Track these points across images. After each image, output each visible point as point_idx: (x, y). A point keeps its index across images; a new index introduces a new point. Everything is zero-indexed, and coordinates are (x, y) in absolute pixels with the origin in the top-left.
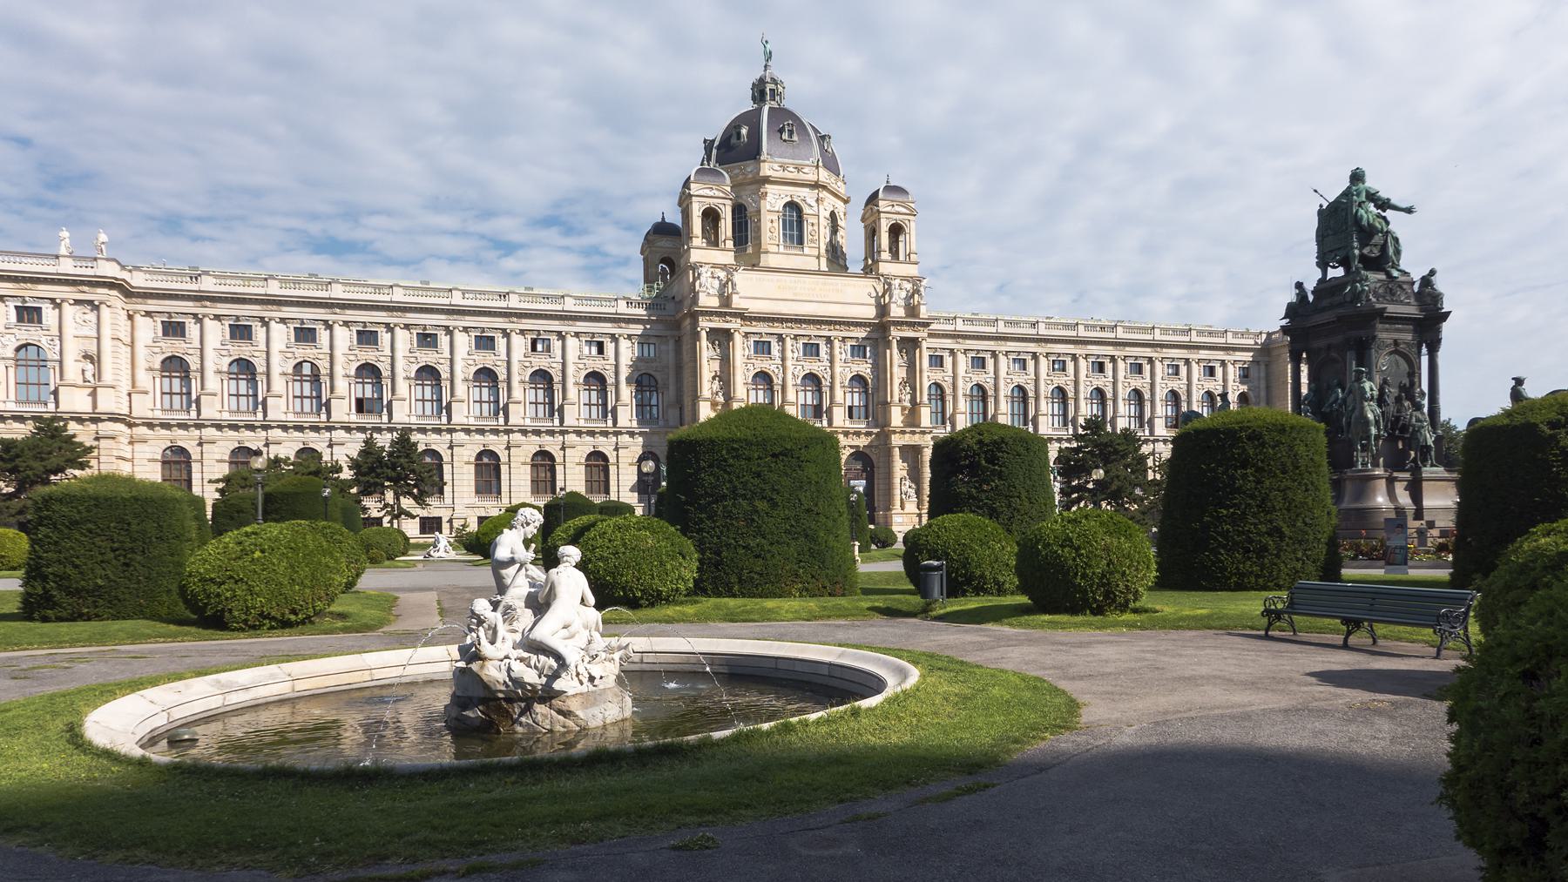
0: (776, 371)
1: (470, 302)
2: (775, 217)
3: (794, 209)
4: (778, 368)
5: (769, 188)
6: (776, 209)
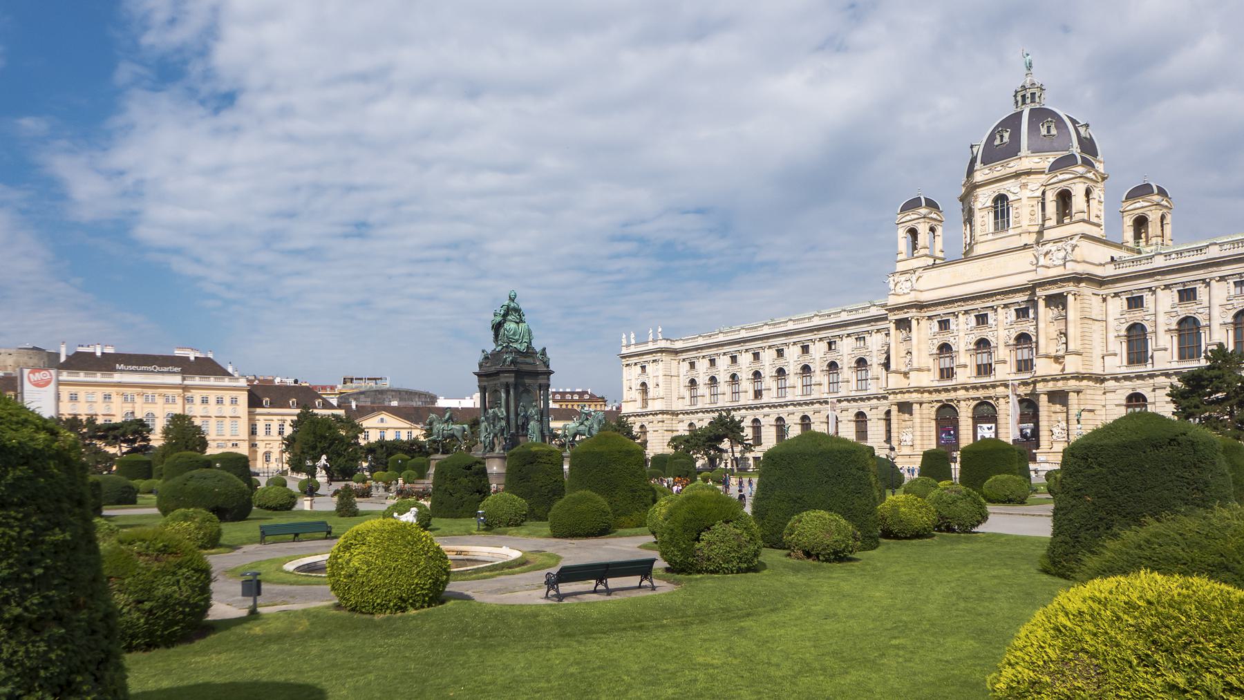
0: (954, 341)
3: (1001, 199)
6: (987, 205)
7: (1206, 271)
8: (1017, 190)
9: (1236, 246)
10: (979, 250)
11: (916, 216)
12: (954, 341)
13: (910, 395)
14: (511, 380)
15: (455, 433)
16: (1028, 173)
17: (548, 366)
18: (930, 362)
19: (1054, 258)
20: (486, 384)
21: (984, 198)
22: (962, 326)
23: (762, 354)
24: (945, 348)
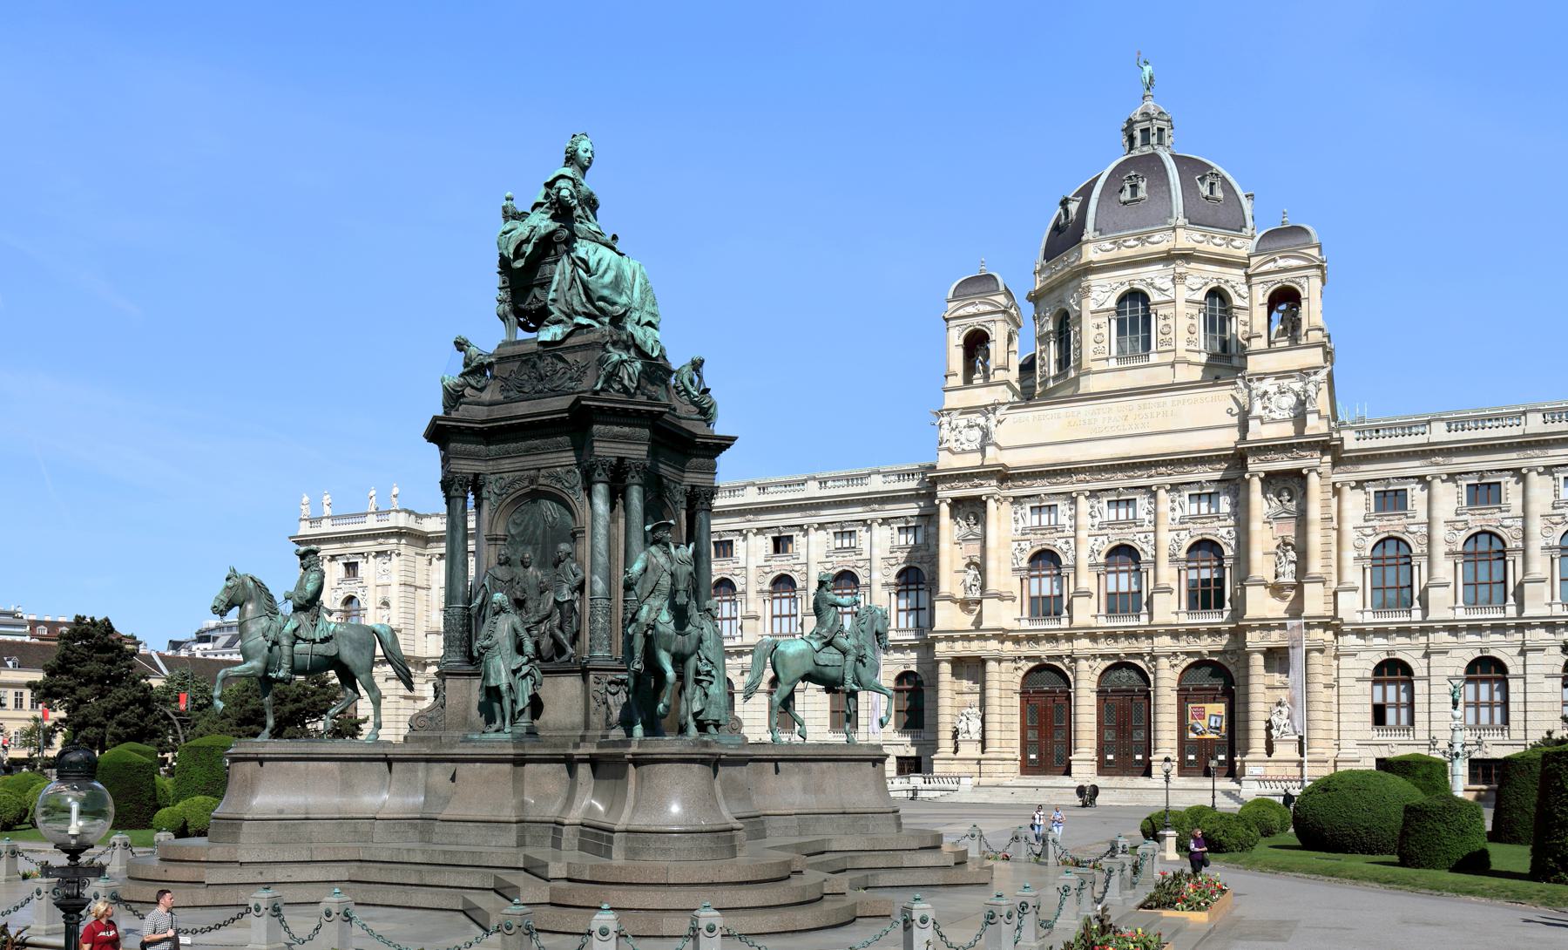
0: (1065, 547)
1: (832, 490)
2: (1103, 319)
4: (1067, 542)
5: (1094, 279)
6: (1106, 306)
7: (1522, 454)
8: (1168, 284)
9: (1407, 431)
10: (1090, 384)
11: (988, 308)
12: (1065, 547)
13: (983, 644)
16: (1188, 257)
18: (1012, 584)
19: (1273, 407)
21: (1103, 292)
22: (1084, 520)
24: (1045, 559)
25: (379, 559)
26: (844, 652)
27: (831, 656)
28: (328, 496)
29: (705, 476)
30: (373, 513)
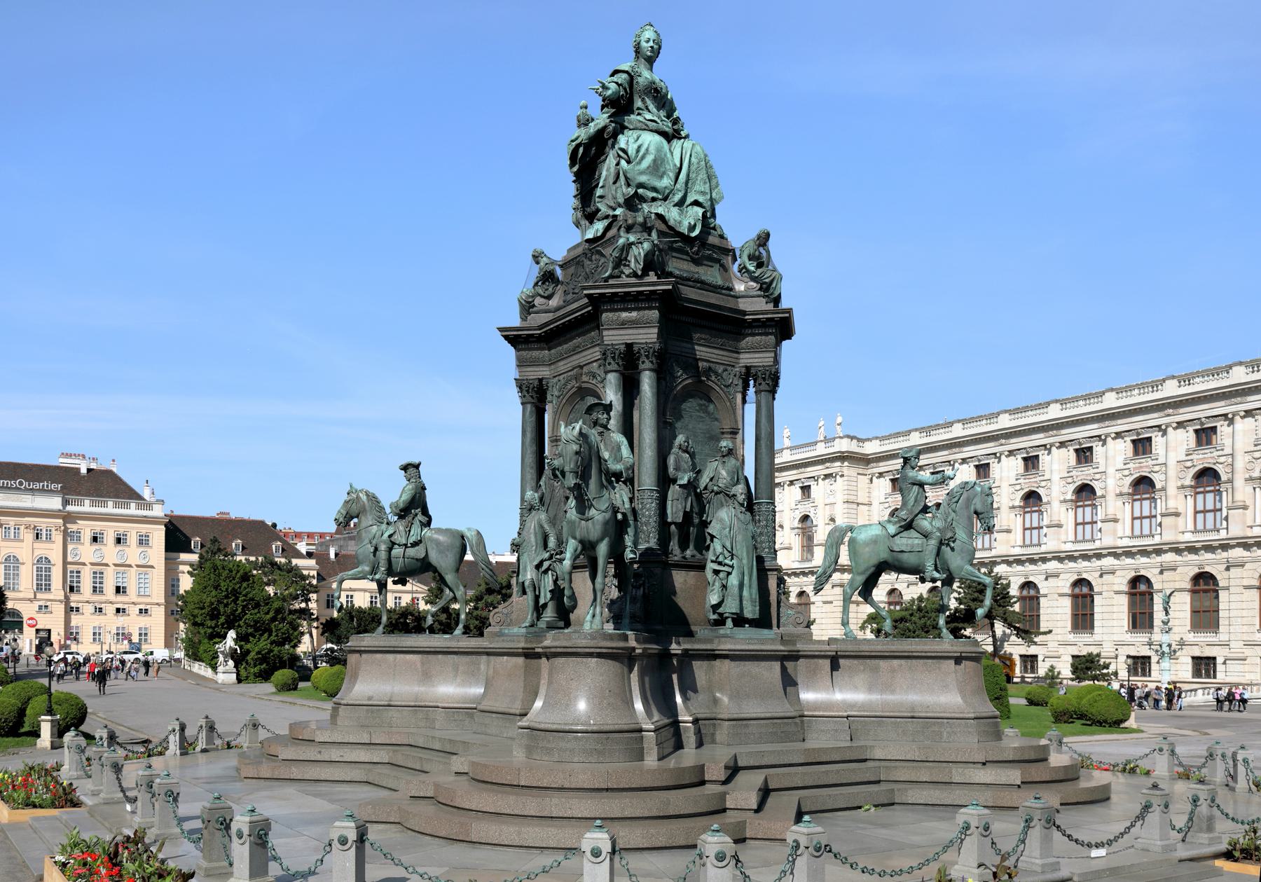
14: (647, 336)
15: (434, 558)
17: (777, 301)
20: (544, 372)
23: (1044, 458)
25: (827, 481)
26: (926, 536)
27: (910, 541)
28: (788, 430)
29: (761, 355)
30: (821, 441)
